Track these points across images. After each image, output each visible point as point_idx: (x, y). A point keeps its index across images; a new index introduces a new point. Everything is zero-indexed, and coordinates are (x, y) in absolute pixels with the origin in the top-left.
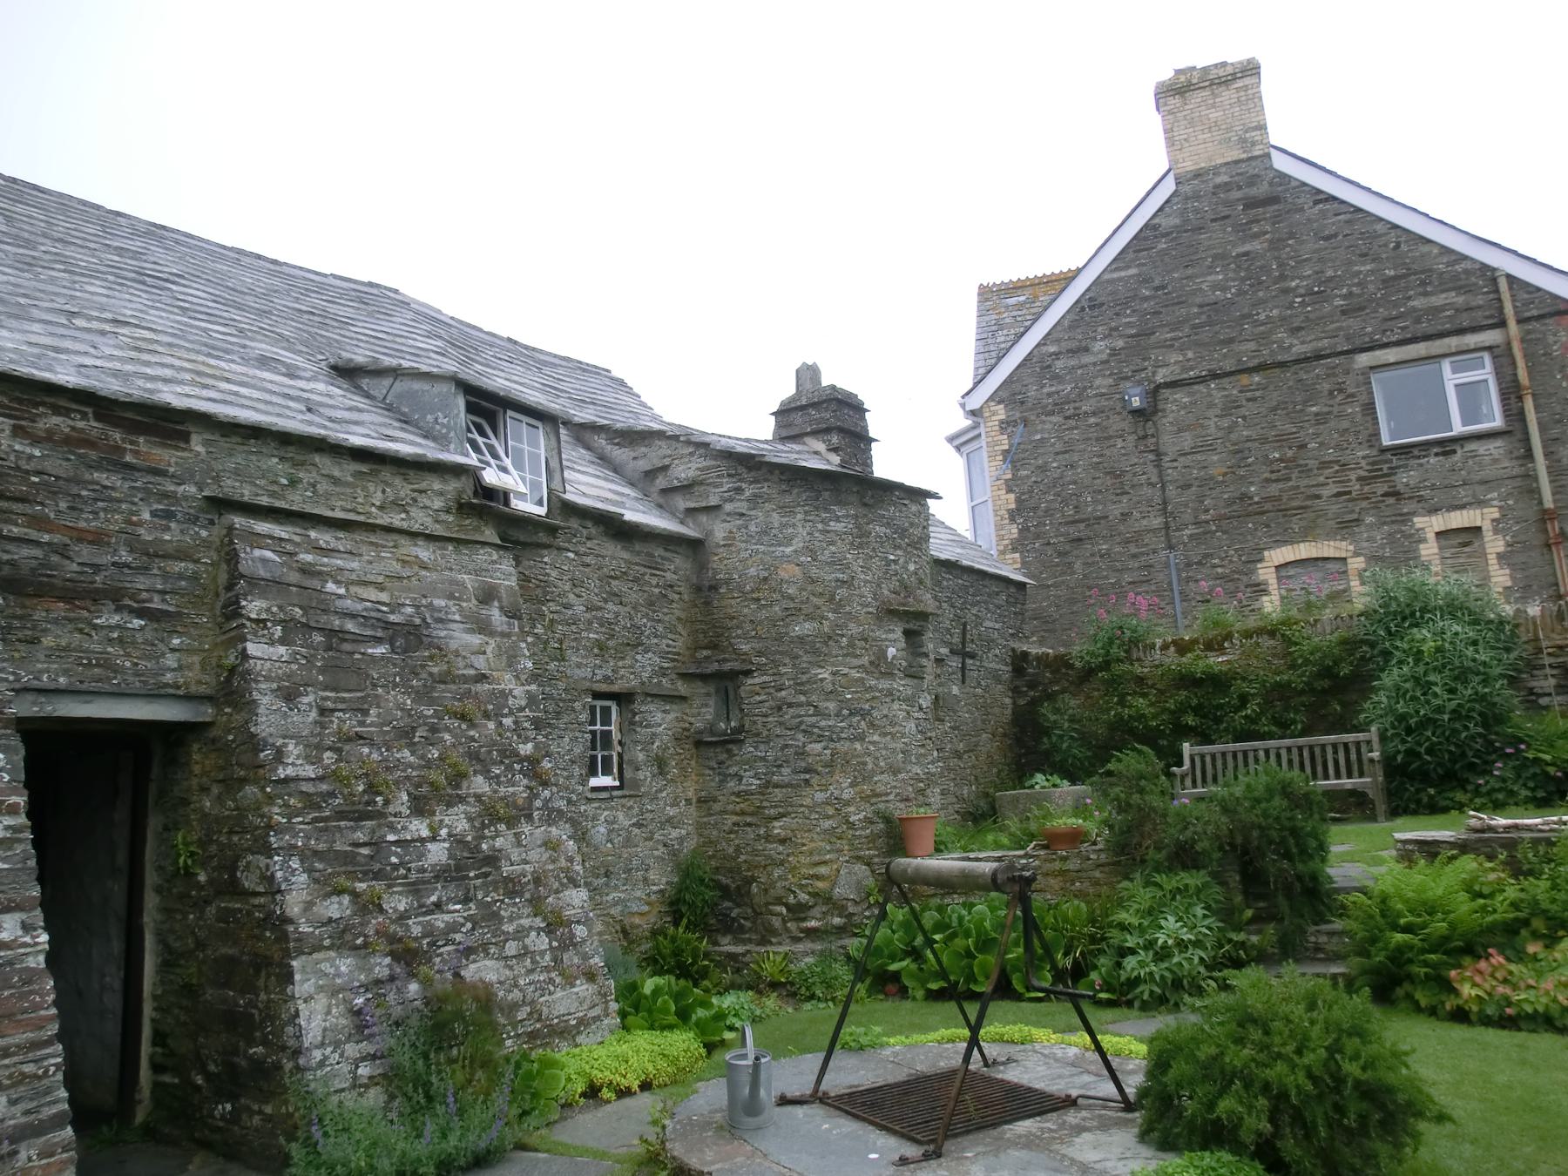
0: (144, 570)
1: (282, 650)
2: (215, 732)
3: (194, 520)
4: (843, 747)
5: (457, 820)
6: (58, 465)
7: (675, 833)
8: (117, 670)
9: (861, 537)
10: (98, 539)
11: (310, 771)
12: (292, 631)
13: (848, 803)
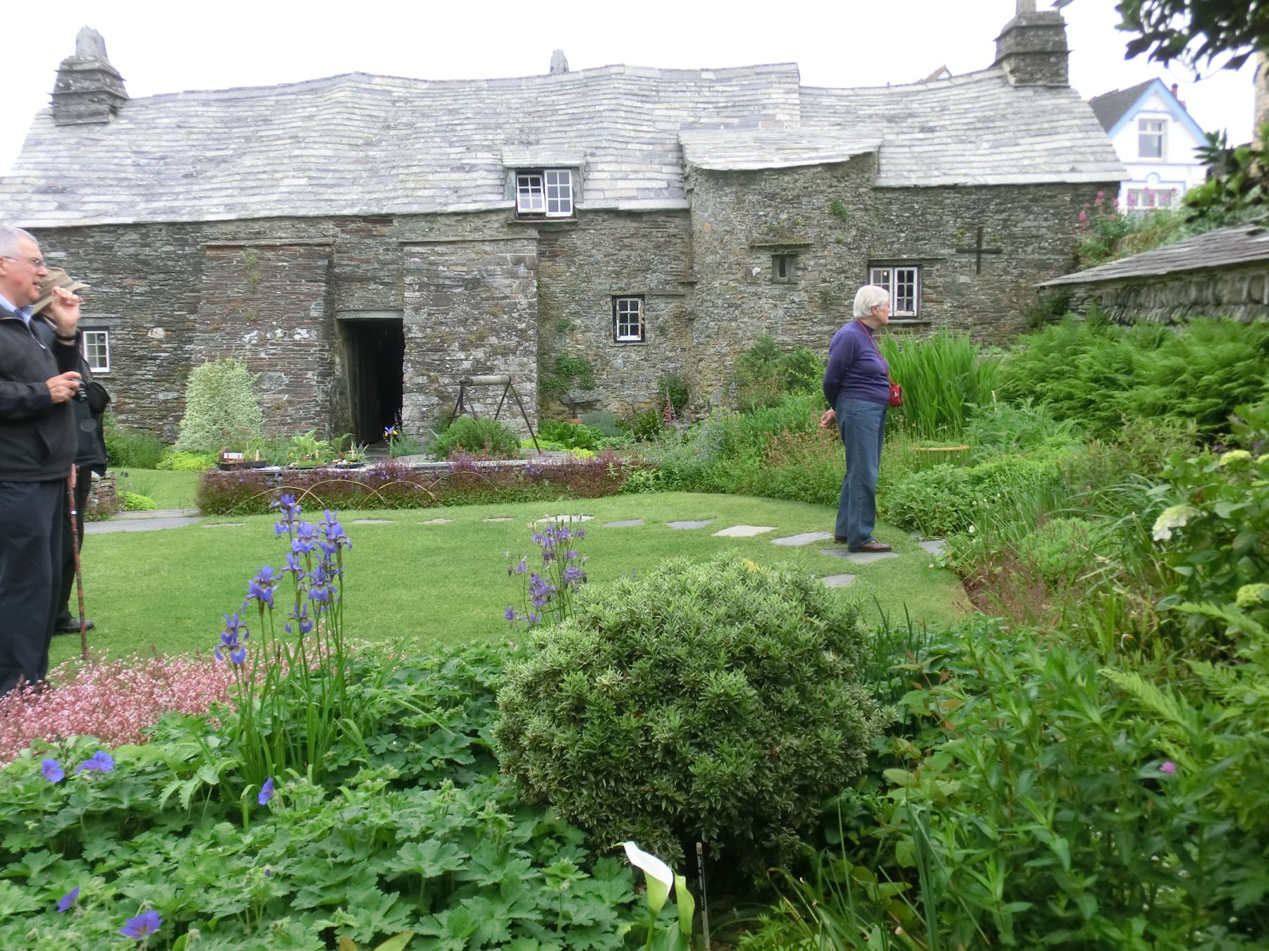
0: (382, 269)
4: (724, 324)
5: (479, 354)
6: (355, 239)
7: (672, 365)
9: (740, 202)
10: (368, 261)
11: (420, 335)
12: (422, 286)
13: (725, 355)
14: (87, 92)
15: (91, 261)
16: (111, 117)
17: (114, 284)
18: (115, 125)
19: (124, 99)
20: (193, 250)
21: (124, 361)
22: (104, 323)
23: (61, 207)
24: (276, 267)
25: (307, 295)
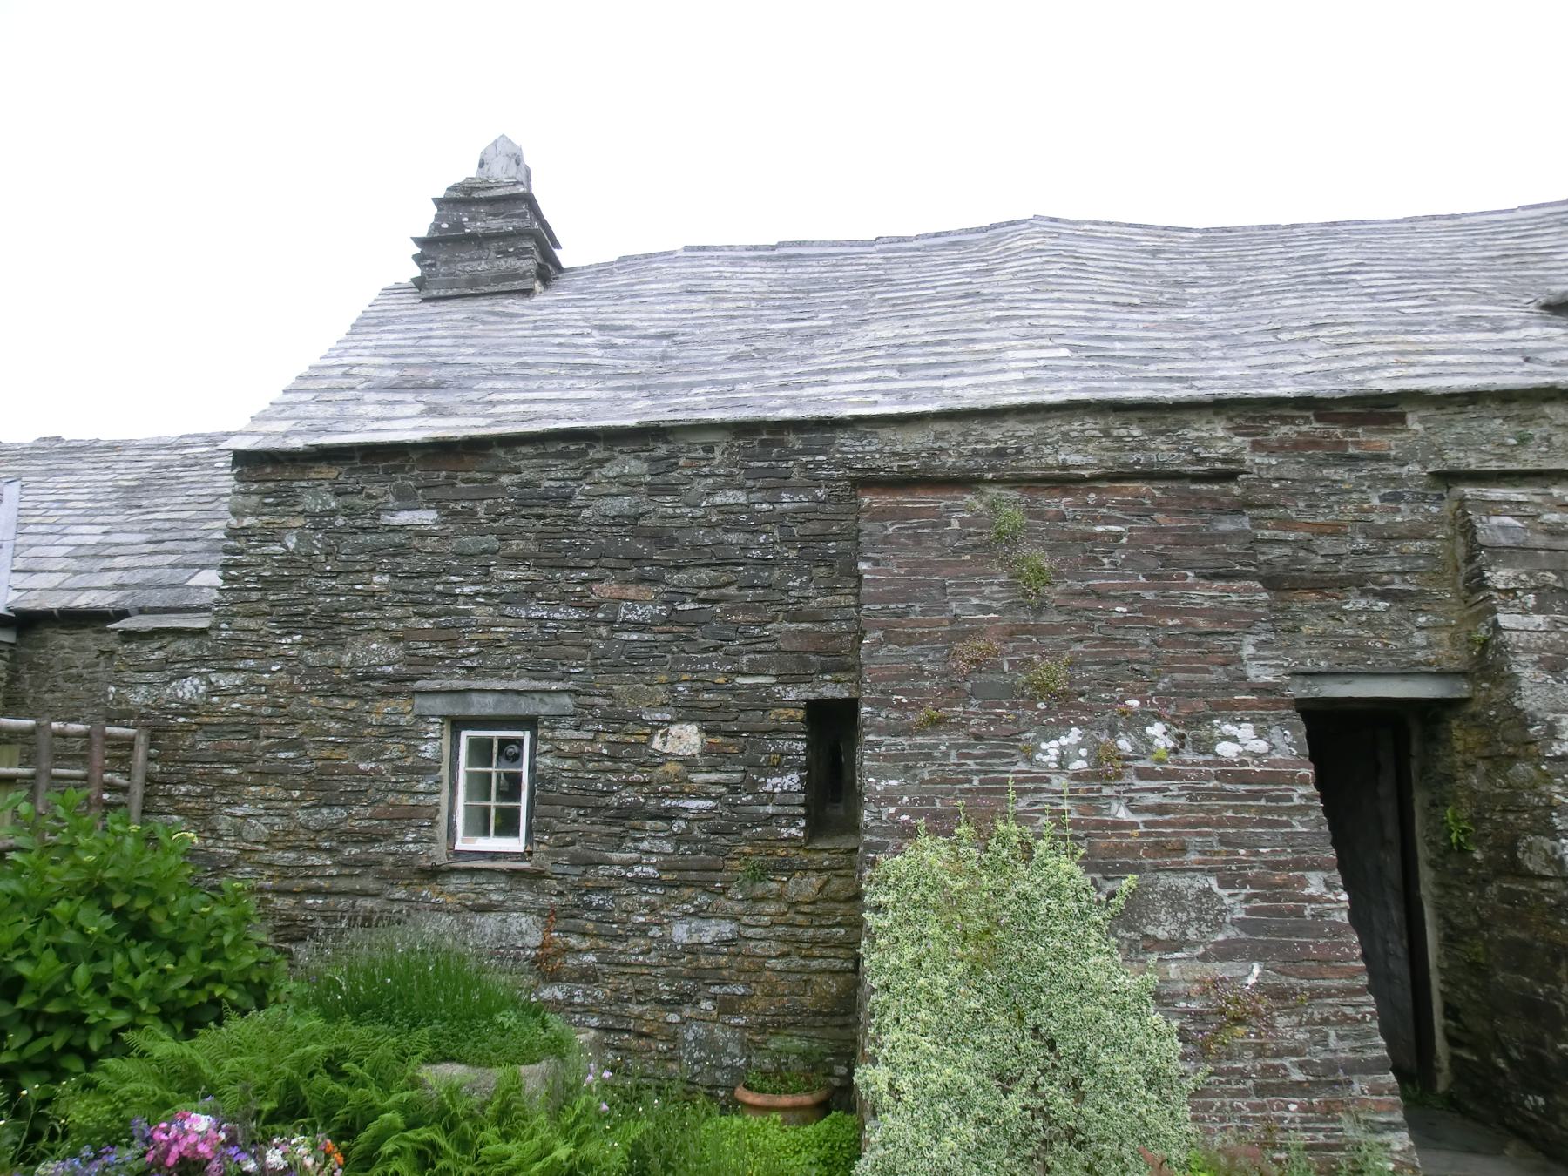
0: (1381, 553)
1: (1538, 619)
2: (1473, 708)
3: (1423, 498)
6: (1292, 470)
8: (1370, 651)
10: (1335, 531)
14: (488, 240)
15: (503, 536)
16: (538, 286)
17: (564, 598)
18: (543, 297)
19: (559, 269)
20: (803, 500)
21: (573, 821)
22: (526, 707)
23: (434, 411)
24: (1088, 537)
25: (1219, 615)
